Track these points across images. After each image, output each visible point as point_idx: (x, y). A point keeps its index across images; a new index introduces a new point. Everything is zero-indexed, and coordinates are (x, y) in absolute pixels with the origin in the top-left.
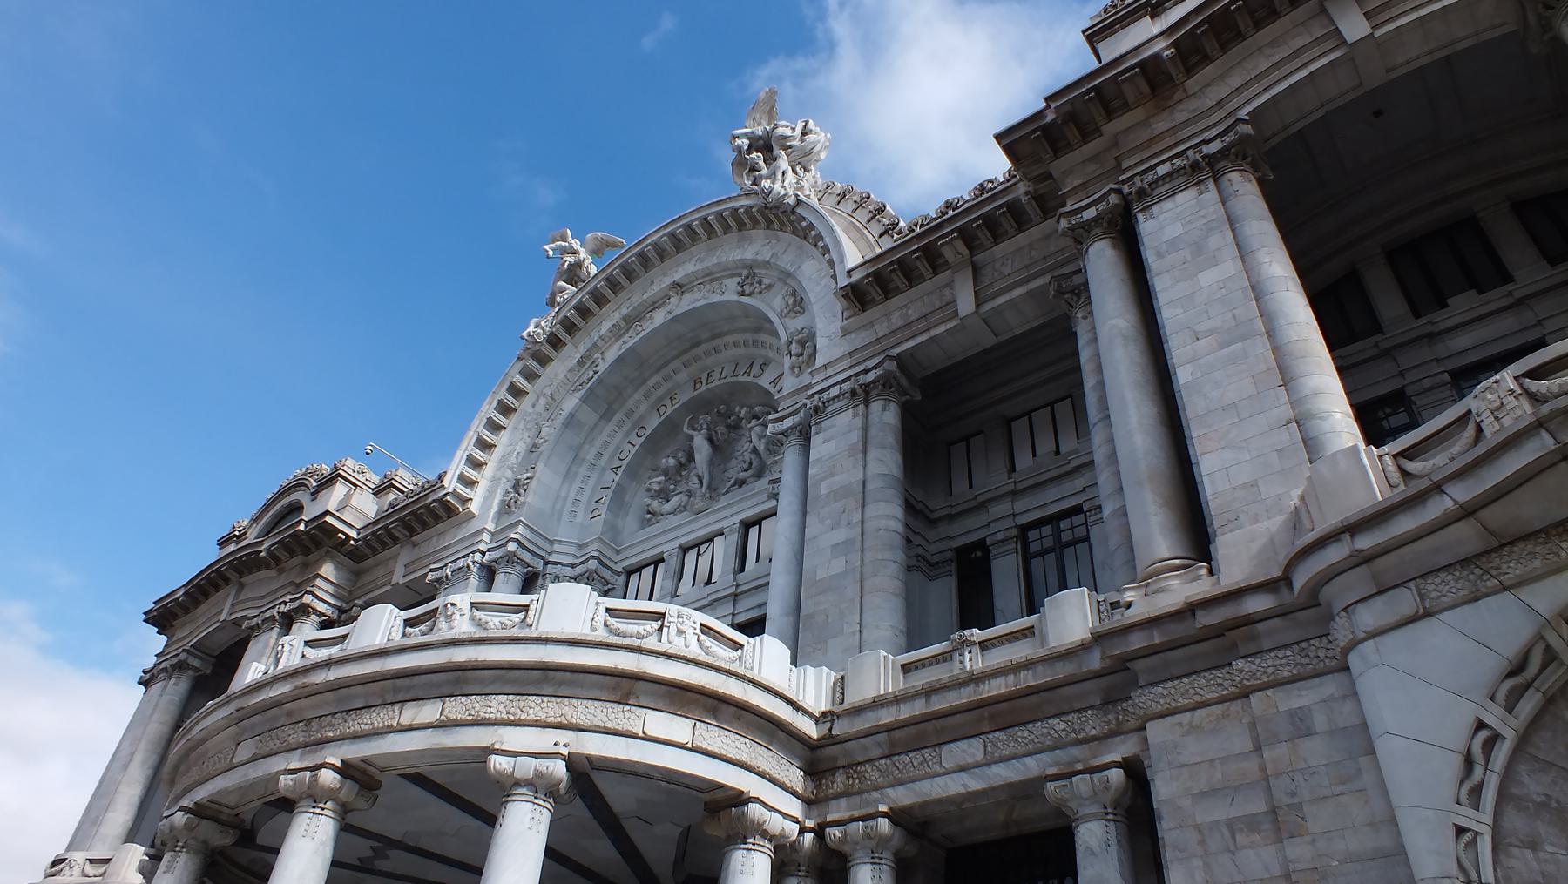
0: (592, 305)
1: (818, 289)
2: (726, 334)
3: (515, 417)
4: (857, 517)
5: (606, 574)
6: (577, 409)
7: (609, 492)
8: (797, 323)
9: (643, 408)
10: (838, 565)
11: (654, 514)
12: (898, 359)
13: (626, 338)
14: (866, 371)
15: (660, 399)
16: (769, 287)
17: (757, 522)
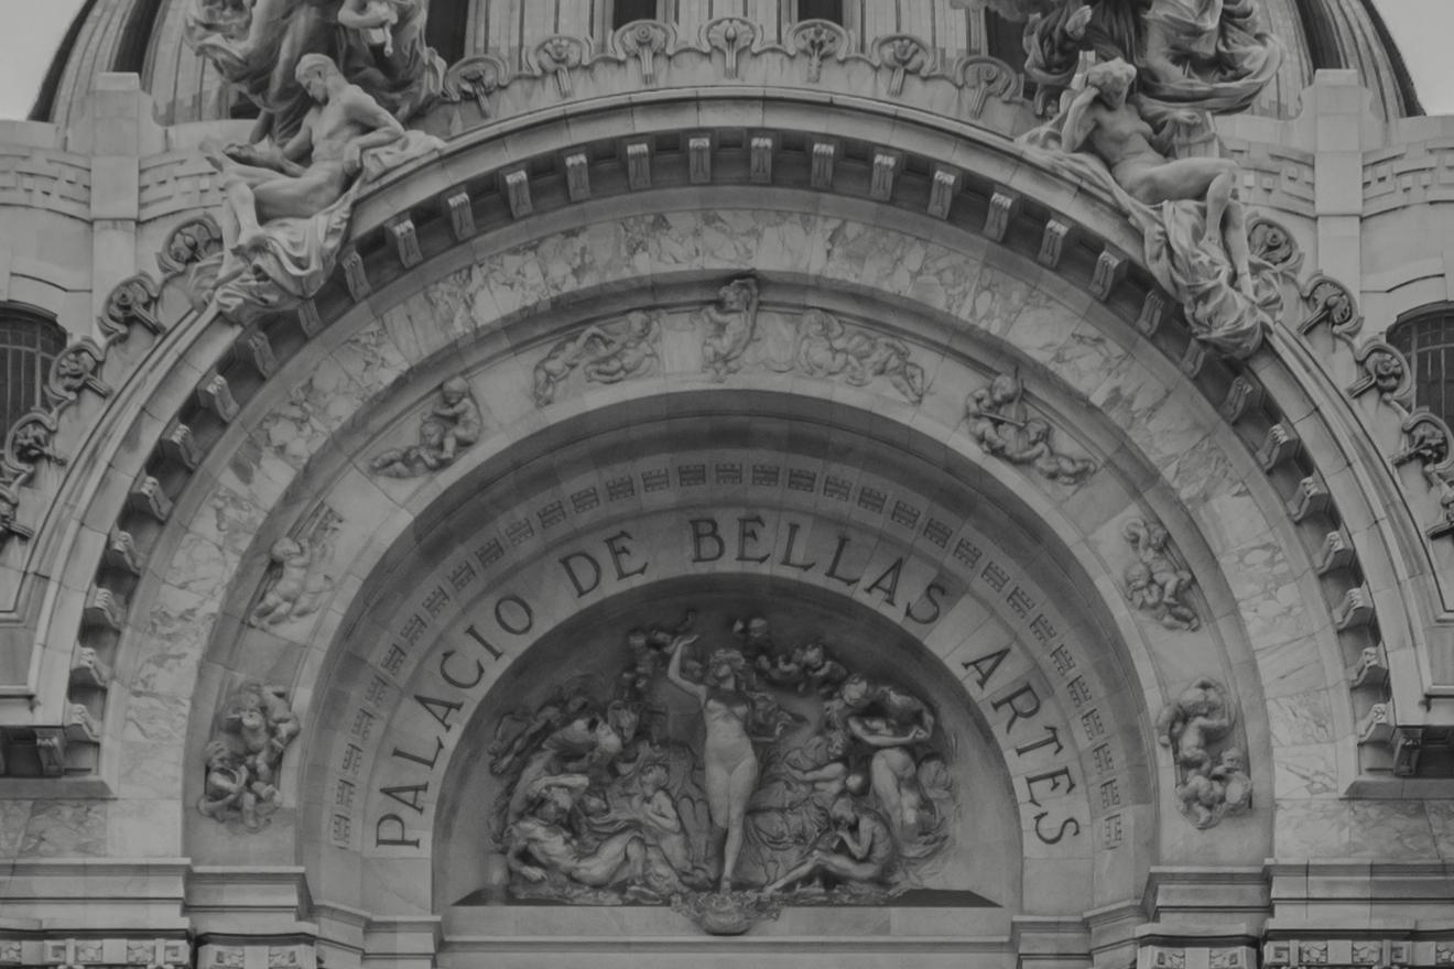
2: (843, 454)
9: (528, 546)
15: (578, 534)
16: (1080, 476)
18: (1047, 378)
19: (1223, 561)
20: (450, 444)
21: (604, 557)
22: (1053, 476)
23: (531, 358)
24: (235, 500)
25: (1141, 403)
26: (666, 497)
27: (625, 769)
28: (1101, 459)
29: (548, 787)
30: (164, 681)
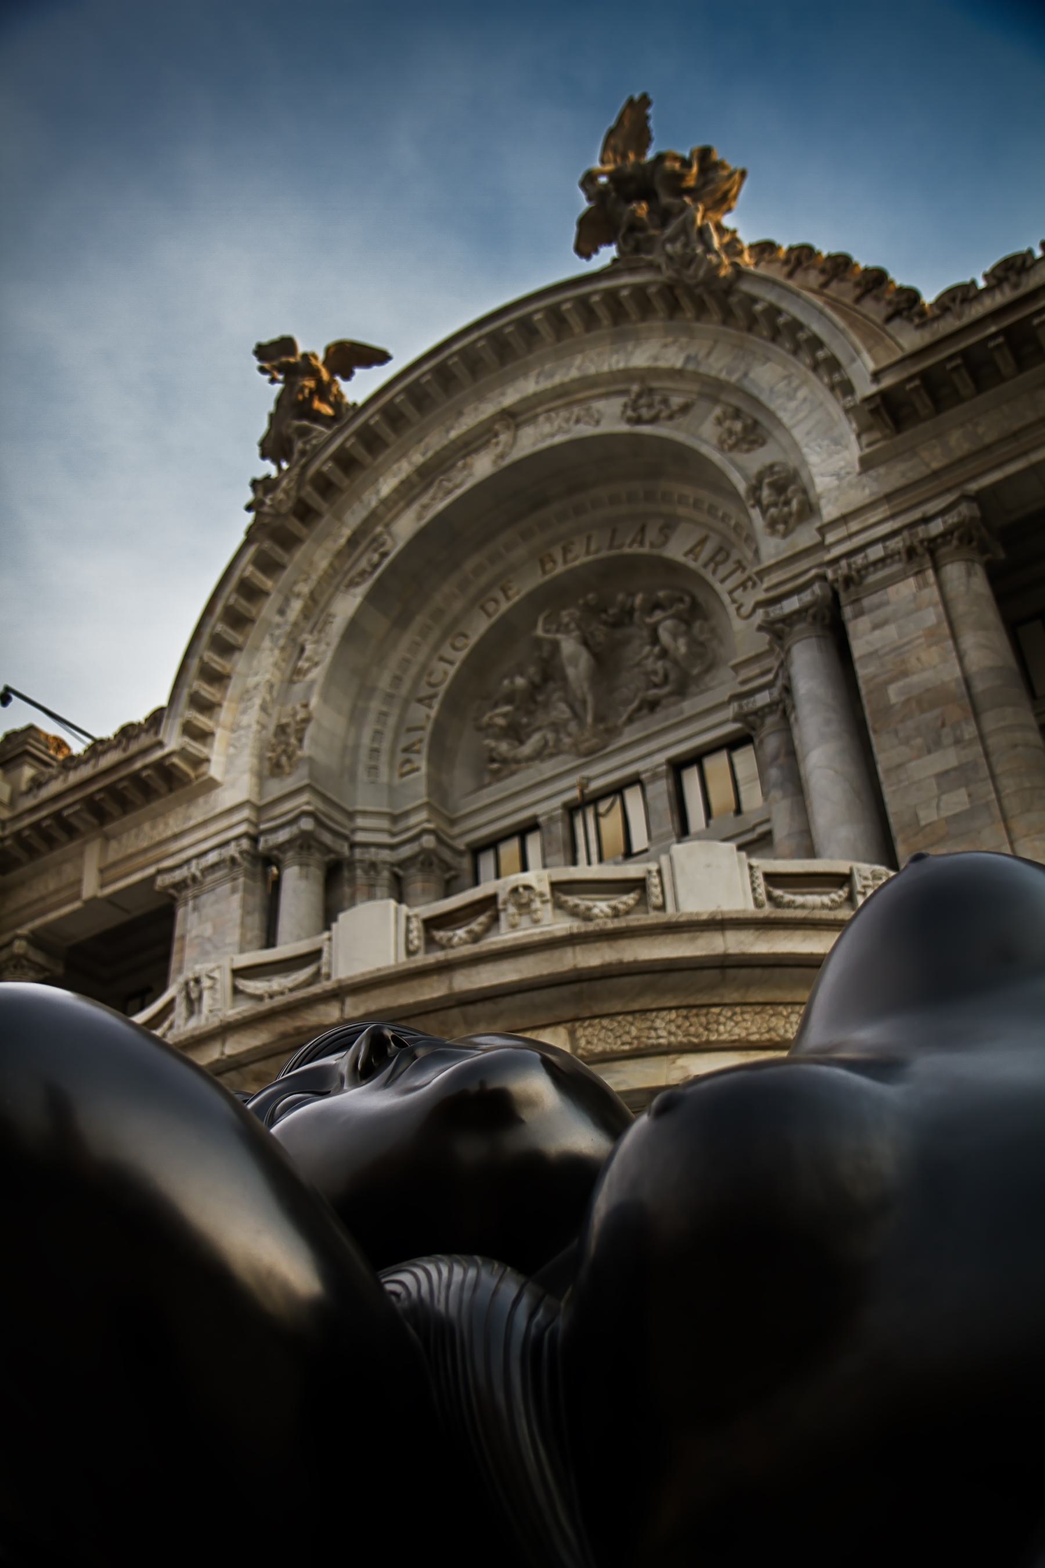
0: (360, 452)
1: (793, 405)
3: (254, 631)
4: (969, 731)
5: (447, 855)
6: (360, 611)
7: (426, 735)
8: (757, 460)
9: (458, 606)
10: (957, 800)
11: (504, 761)
12: (977, 498)
13: (425, 499)
14: (926, 520)
15: (483, 592)
16: (685, 409)
17: (696, 759)
18: (653, 372)
19: (764, 398)
20: (376, 557)
21: (500, 596)
22: (671, 417)
23: (416, 507)
24: (278, 626)
25: (702, 354)
26: (521, 552)
27: (540, 698)
28: (694, 396)
29: (491, 718)
30: (245, 720)
